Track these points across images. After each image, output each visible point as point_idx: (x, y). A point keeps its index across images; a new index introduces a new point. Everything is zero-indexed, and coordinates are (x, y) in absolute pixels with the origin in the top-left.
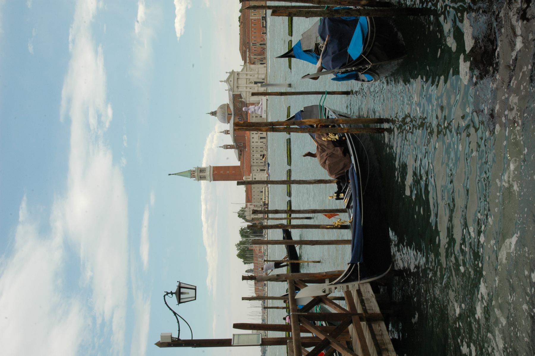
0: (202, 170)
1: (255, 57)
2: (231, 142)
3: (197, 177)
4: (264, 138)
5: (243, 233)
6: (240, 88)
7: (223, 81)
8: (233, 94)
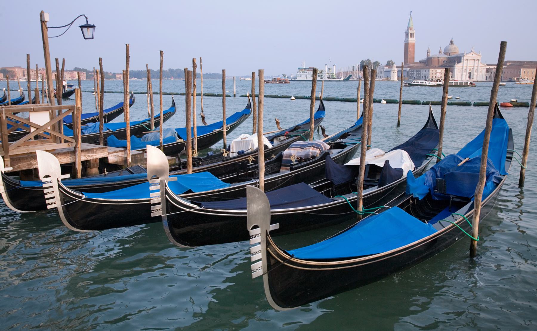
0: (412, 35)
2: (431, 55)
5: (376, 63)
6: (466, 61)
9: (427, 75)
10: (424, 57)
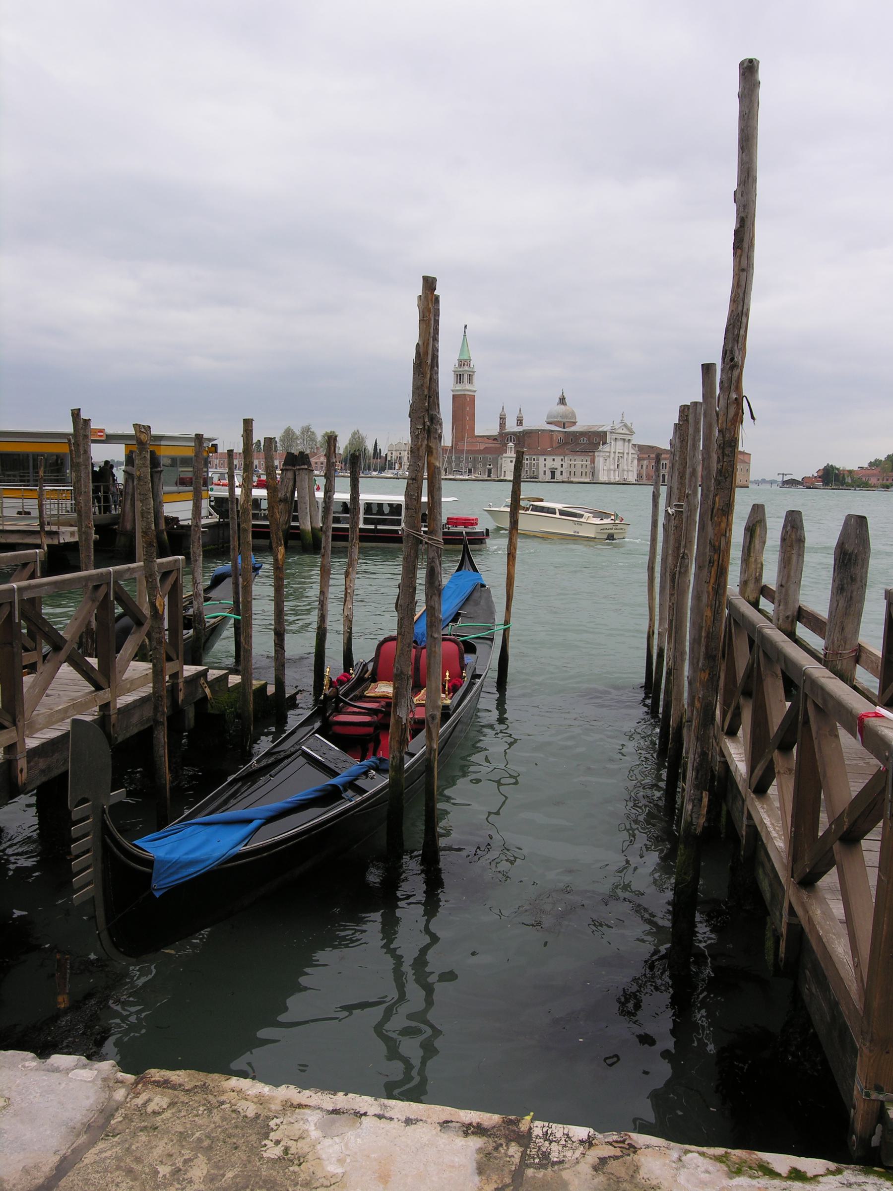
1: (645, 467)
3: (460, 369)
4: (553, 477)
7: (623, 417)
8: (607, 431)
9: (560, 469)
10: (494, 430)
